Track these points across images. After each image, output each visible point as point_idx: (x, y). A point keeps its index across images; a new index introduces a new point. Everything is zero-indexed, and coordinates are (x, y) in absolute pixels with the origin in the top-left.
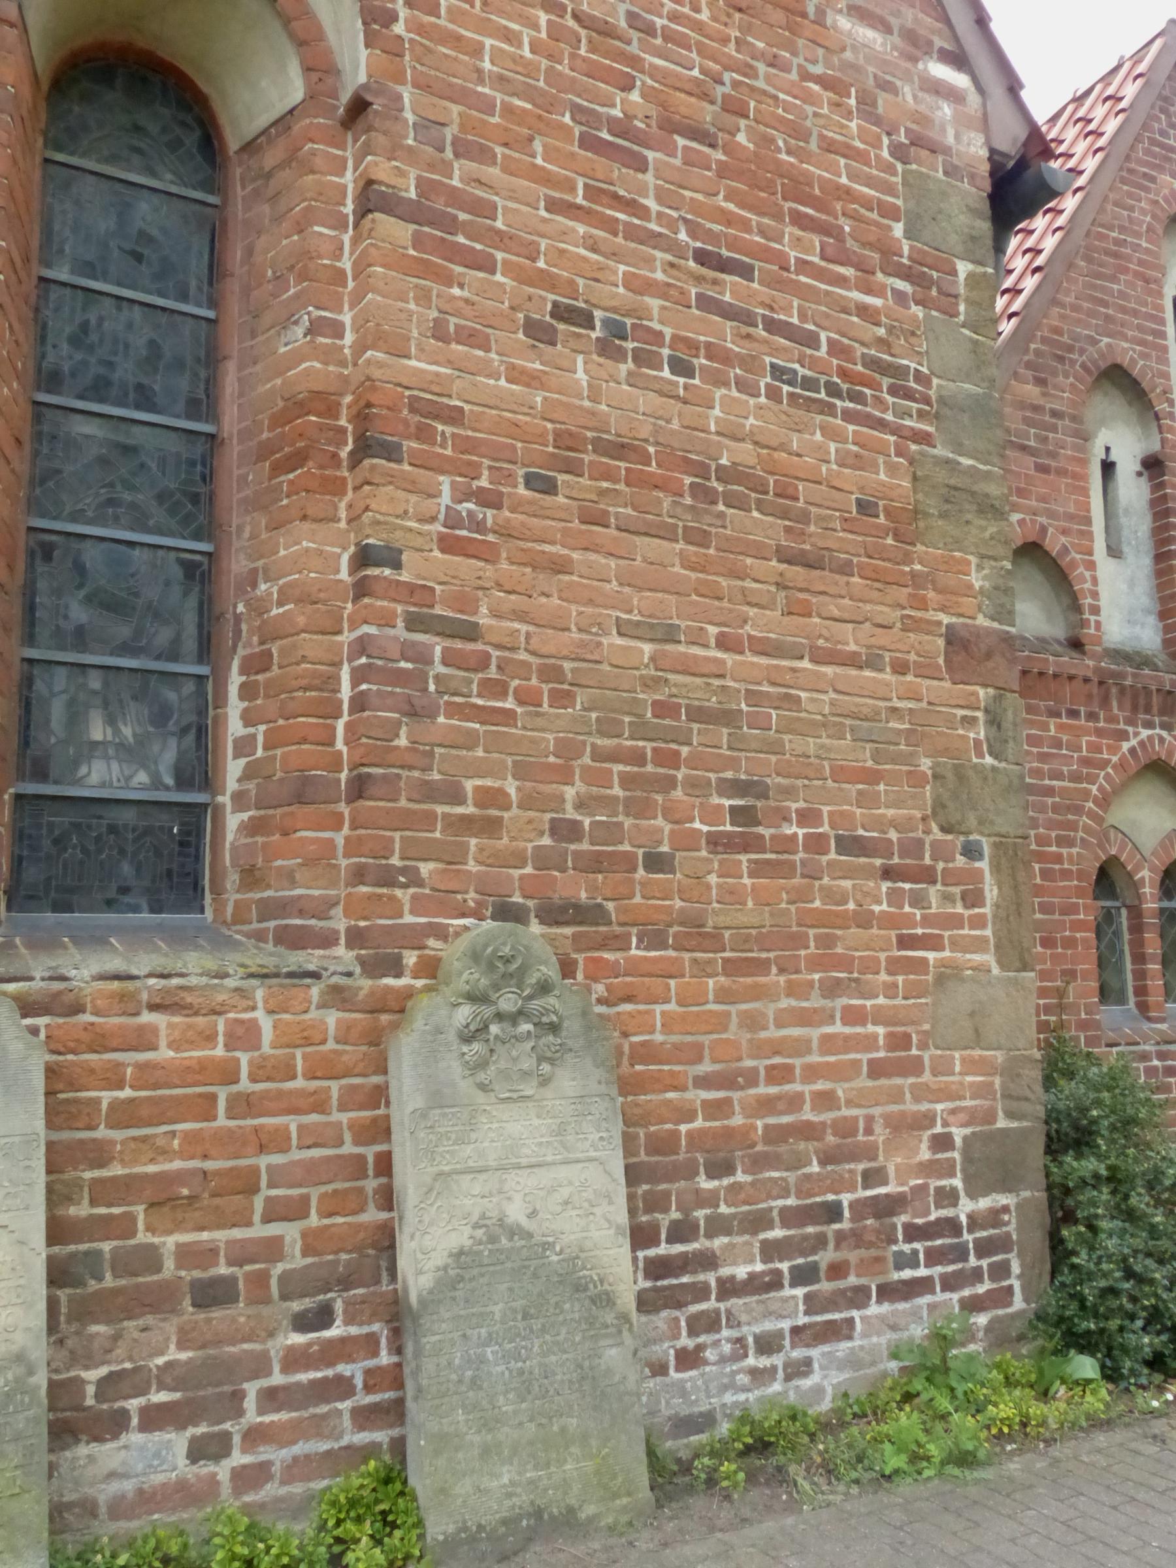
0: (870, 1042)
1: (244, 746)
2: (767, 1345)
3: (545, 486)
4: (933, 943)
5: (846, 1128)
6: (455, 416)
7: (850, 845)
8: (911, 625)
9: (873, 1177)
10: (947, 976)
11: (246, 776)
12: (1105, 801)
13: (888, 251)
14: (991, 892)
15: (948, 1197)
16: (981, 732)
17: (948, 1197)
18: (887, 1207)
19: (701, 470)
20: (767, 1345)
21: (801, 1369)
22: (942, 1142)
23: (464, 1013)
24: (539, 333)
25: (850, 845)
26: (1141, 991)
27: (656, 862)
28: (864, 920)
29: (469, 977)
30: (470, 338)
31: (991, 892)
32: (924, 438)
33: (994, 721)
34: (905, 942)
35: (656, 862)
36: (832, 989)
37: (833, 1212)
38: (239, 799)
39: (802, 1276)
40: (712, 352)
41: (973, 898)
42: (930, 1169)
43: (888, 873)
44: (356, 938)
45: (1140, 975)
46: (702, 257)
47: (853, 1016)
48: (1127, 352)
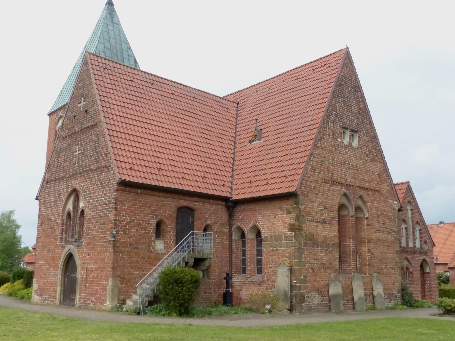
0: (392, 282)
1: (359, 261)
2: (387, 302)
3: (376, 243)
4: (395, 275)
5: (391, 288)
6: (372, 239)
7: (391, 268)
8: (394, 250)
9: (392, 292)
10: (396, 277)
11: (359, 263)
12: (402, 262)
13: (392, 219)
14: (398, 271)
15: (396, 294)
16: (397, 258)
17: (396, 294)
18: (393, 294)
19: (383, 240)
20: (387, 302)
21: (389, 304)
22: (396, 290)
23: (376, 279)
24: (376, 232)
25: (391, 268)
26: (404, 279)
27: (382, 269)
28: (392, 273)
29: (376, 277)
30: (373, 234)
31: (398, 271)
32: (394, 235)
33: (399, 257)
34: (394, 275)
35: (382, 269)
36: (390, 278)
37: (390, 294)
38: (359, 265)
39: (389, 298)
40: (384, 231)
41: (397, 272)
42: (395, 292)
43: (393, 270)
44: (368, 274)
45: (404, 277)
46: (383, 224)
47: (391, 280)
48: (404, 217)
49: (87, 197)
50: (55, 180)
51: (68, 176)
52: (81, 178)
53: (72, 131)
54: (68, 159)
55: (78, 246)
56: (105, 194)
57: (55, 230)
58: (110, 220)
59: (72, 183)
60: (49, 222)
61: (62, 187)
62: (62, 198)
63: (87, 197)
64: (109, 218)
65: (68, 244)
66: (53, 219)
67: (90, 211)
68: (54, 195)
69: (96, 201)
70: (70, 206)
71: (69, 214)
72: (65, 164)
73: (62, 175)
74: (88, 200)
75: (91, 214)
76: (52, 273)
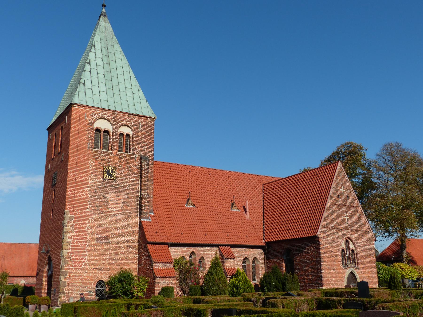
49: (358, 244)
50: (332, 228)
51: (342, 228)
52: (353, 233)
53: (339, 203)
54: (340, 219)
55: (356, 269)
56: (368, 244)
57: (337, 258)
58: (373, 258)
59: (346, 233)
60: (330, 253)
61: (338, 234)
62: (340, 240)
63: (358, 244)
64: (373, 257)
65: (350, 267)
66: (334, 251)
67: (361, 251)
68: (333, 237)
69: (364, 247)
70: (343, 245)
71: (343, 250)
72: (339, 221)
73: (338, 227)
74: (359, 245)
75: (361, 253)
76: (339, 283)
